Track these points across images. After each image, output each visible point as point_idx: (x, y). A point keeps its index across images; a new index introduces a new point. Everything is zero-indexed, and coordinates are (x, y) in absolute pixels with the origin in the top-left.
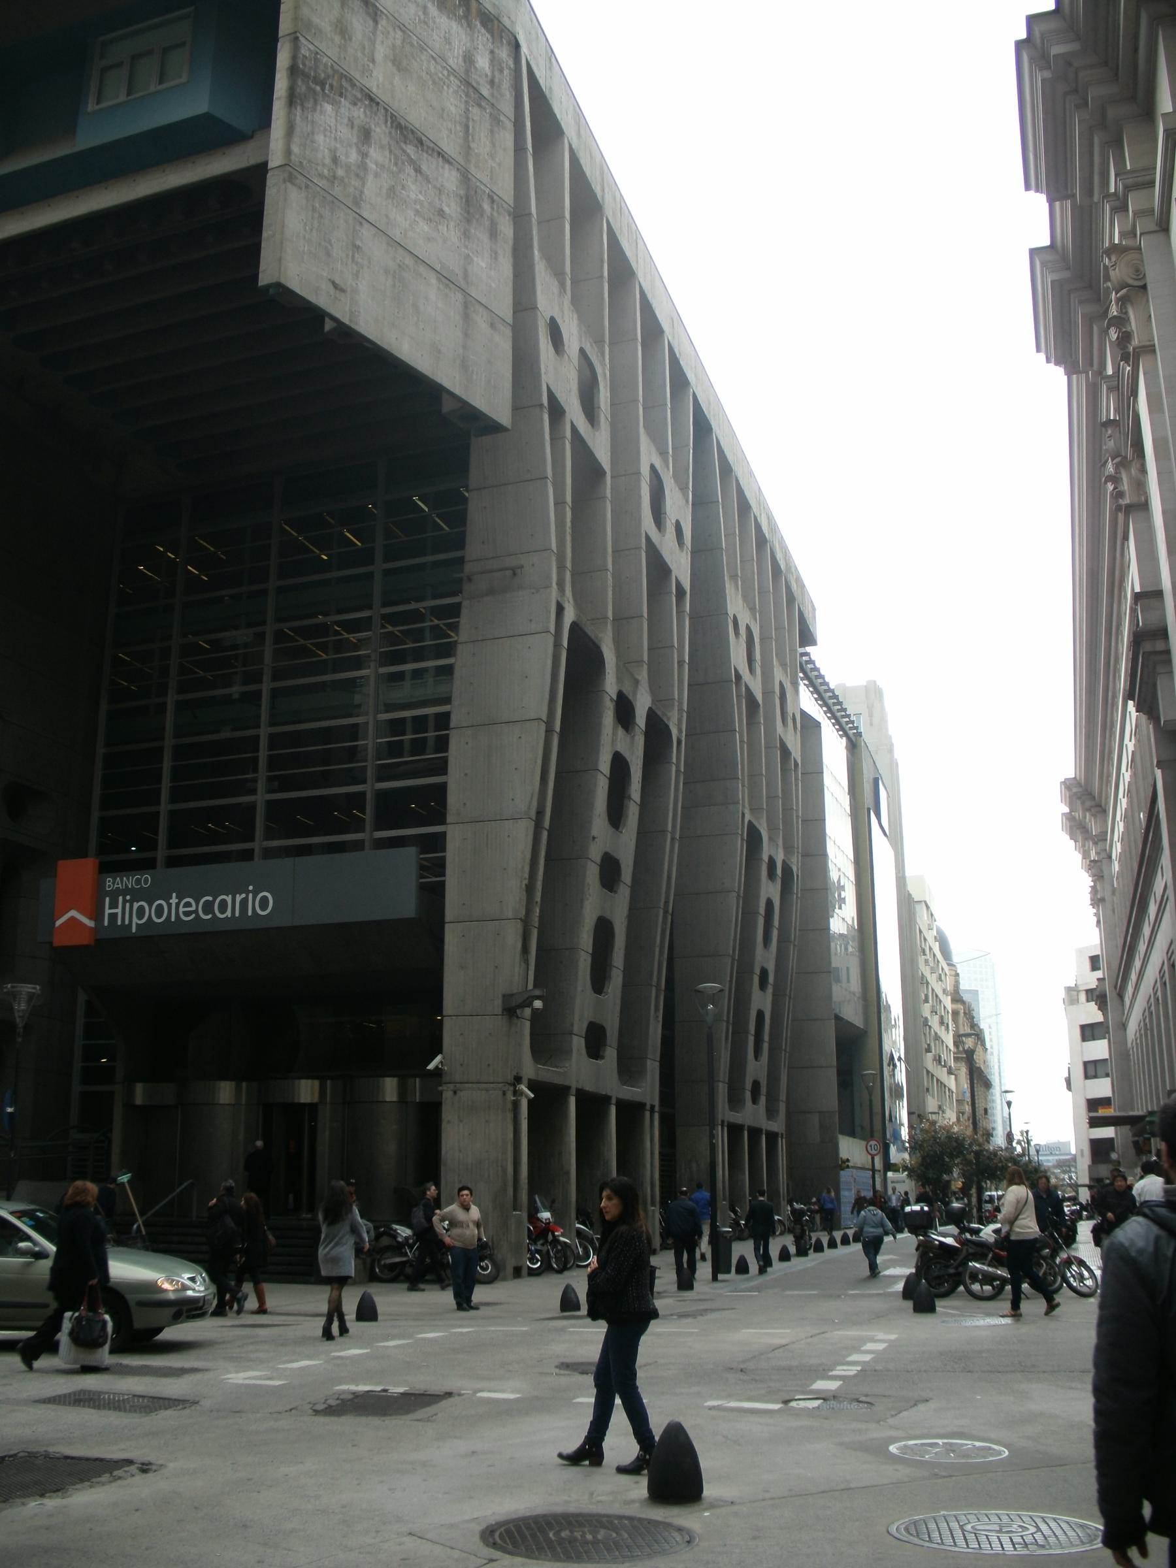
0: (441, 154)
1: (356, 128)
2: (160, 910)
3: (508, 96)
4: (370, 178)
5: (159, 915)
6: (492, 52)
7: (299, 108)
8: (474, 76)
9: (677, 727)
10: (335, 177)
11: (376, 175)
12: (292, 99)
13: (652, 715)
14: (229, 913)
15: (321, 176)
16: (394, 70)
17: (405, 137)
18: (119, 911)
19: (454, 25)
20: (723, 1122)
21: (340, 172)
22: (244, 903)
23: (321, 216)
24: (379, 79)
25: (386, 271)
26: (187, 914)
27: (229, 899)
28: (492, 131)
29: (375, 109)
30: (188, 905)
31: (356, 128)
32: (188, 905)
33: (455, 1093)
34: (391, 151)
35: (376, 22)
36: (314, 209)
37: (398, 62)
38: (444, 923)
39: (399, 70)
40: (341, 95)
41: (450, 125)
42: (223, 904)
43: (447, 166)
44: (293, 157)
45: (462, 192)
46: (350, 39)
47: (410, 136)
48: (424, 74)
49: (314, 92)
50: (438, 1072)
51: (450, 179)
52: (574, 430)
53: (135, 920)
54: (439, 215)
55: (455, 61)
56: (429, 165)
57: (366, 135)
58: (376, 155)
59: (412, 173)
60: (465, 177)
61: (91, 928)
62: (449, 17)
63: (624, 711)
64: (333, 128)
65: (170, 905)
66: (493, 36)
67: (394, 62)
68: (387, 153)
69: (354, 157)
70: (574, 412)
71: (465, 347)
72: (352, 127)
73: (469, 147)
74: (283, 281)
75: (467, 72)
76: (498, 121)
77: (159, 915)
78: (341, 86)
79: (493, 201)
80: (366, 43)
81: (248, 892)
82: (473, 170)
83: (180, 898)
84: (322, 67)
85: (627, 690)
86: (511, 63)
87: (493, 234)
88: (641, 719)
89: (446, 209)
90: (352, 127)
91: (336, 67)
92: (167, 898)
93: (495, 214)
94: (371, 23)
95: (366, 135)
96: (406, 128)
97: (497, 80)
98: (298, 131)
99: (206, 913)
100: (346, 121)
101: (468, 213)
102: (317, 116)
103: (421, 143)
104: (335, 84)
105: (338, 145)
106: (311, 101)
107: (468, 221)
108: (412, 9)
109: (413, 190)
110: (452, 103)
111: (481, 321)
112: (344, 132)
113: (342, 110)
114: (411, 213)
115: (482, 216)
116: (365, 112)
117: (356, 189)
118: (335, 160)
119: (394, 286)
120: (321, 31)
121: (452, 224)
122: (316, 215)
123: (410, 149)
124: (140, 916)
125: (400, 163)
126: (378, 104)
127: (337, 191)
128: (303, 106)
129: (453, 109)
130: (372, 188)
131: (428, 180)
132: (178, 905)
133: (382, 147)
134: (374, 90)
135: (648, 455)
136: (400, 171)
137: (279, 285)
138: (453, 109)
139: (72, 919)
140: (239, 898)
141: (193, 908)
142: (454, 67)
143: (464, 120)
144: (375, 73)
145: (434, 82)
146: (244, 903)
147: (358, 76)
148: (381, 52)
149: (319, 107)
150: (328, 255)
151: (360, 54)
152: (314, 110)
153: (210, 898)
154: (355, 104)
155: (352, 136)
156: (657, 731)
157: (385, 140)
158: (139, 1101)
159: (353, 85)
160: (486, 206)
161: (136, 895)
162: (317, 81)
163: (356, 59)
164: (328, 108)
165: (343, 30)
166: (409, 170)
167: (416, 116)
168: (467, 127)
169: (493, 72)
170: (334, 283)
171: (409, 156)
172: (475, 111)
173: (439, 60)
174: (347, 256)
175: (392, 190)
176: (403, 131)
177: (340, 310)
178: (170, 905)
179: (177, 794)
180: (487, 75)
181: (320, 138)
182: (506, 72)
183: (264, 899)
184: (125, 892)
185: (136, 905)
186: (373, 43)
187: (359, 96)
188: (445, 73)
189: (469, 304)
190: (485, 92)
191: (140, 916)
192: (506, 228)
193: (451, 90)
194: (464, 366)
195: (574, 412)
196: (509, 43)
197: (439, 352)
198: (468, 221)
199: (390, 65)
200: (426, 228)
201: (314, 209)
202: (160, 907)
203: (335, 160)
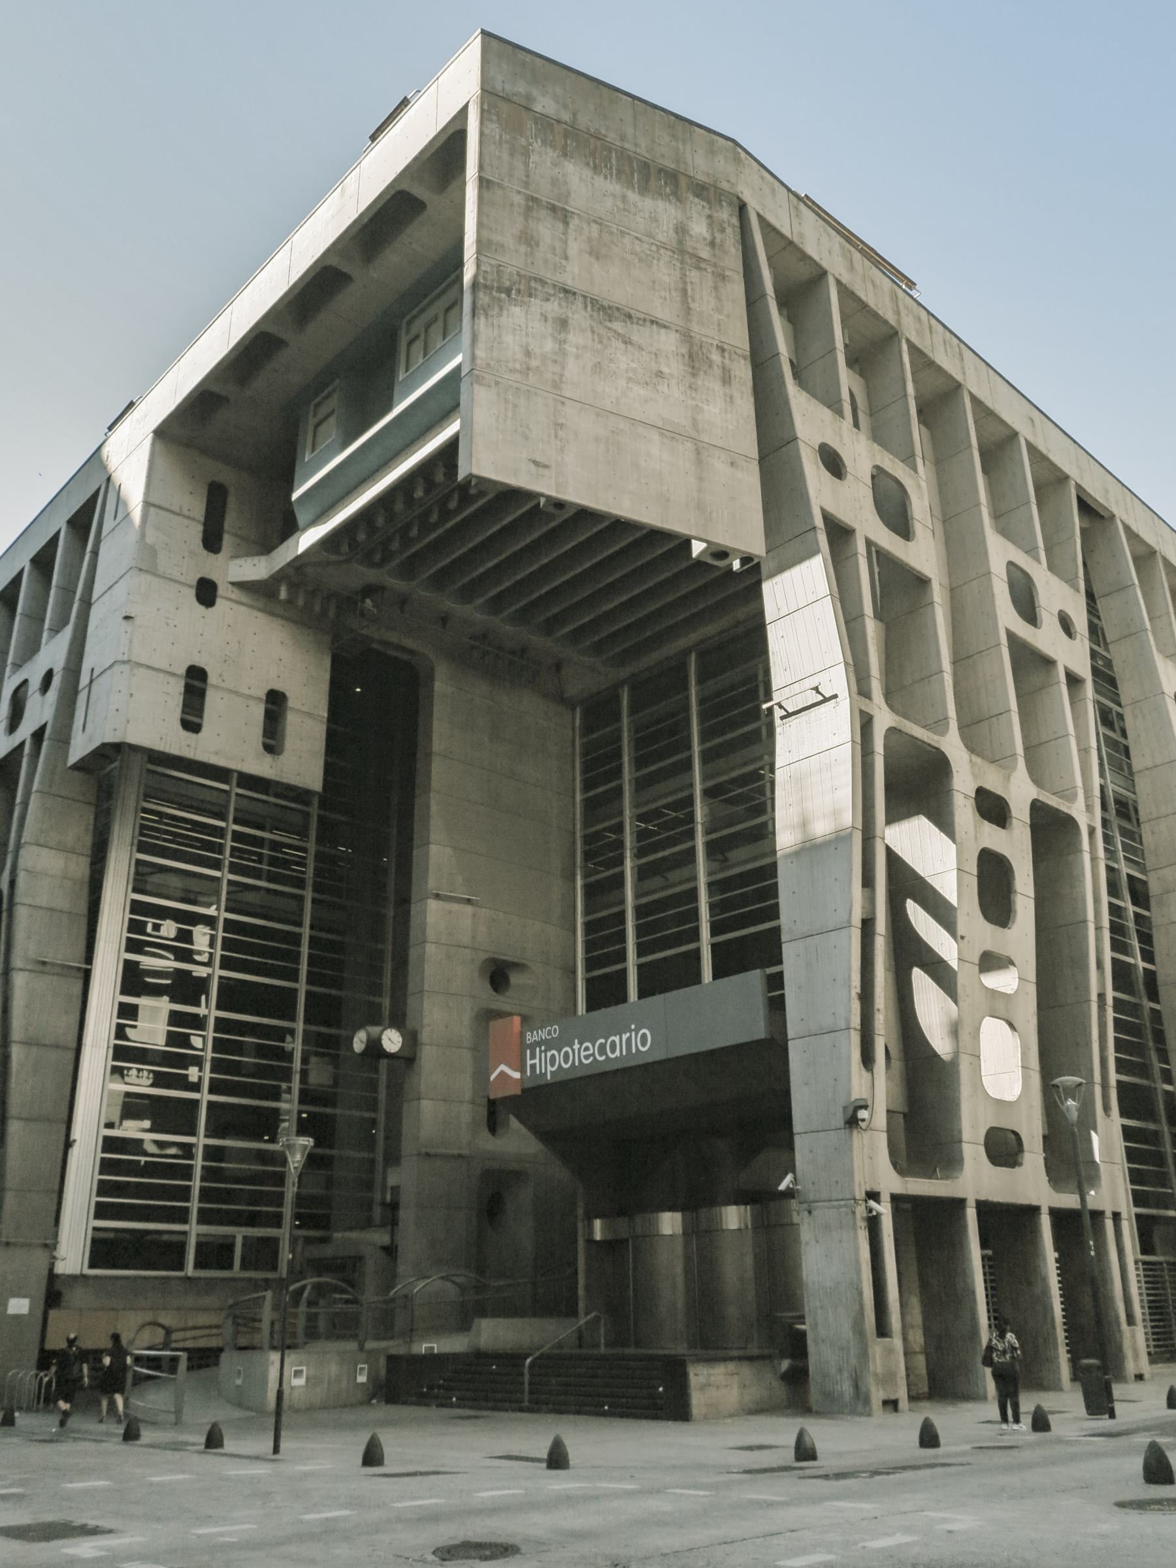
1: (550, 320)
3: (733, 250)
6: (709, 217)
7: (482, 318)
8: (689, 244)
9: (1084, 813)
10: (528, 369)
11: (577, 357)
13: (1037, 808)
14: (618, 1053)
17: (610, 316)
18: (537, 1061)
19: (661, 204)
21: (534, 363)
22: (629, 1040)
23: (516, 406)
24: (574, 274)
25: (597, 440)
26: (587, 1057)
27: (617, 1039)
28: (716, 288)
29: (571, 298)
30: (587, 1049)
31: (550, 320)
32: (587, 1049)
33: (810, 1212)
34: (593, 332)
35: (566, 223)
36: (506, 401)
37: (595, 253)
38: (786, 1041)
39: (597, 258)
40: (530, 295)
41: (663, 294)
42: (613, 1044)
43: (663, 331)
44: (478, 362)
45: (684, 350)
46: (537, 245)
47: (616, 313)
48: (628, 257)
49: (499, 300)
50: (790, 1194)
51: (668, 342)
52: (869, 543)
53: (549, 1068)
54: (657, 376)
55: (665, 233)
56: (638, 334)
57: (563, 324)
59: (622, 346)
60: (687, 336)
61: (516, 1080)
62: (653, 198)
63: (993, 808)
64: (524, 326)
65: (573, 1051)
66: (709, 202)
67: (590, 254)
68: (589, 334)
69: (549, 346)
70: (869, 526)
71: (700, 491)
72: (546, 320)
73: (689, 309)
74: (475, 471)
75: (680, 242)
76: (724, 278)
77: (566, 1062)
78: (530, 288)
79: (723, 350)
80: (557, 244)
81: (630, 1031)
82: (695, 327)
83: (581, 1043)
84: (506, 277)
85: (993, 783)
86: (735, 221)
87: (726, 379)
88: (1020, 813)
89: (666, 370)
90: (546, 320)
91: (522, 272)
92: (571, 1045)
93: (727, 361)
94: (561, 225)
96: (610, 307)
97: (718, 241)
98: (482, 338)
99: (601, 1055)
100: (538, 316)
101: (693, 368)
102: (504, 320)
103: (630, 317)
104: (522, 287)
105: (530, 340)
106: (496, 309)
107: (694, 375)
108: (609, 202)
109: (623, 360)
110: (665, 271)
111: (719, 465)
112: (536, 326)
113: (533, 309)
114: (622, 383)
115: (711, 367)
116: (560, 305)
117: (554, 374)
118: (528, 354)
119: (608, 451)
120: (503, 246)
121: (673, 382)
122: (510, 406)
123: (617, 326)
124: (552, 1065)
125: (605, 341)
126: (575, 294)
128: (486, 315)
129: (667, 279)
130: (572, 369)
131: (640, 348)
132: (579, 1050)
133: (583, 330)
134: (569, 282)
135: (1000, 553)
136: (606, 348)
137: (471, 475)
138: (667, 279)
139: (502, 1072)
140: (625, 1037)
141: (591, 1052)
142: (664, 240)
143: (681, 286)
144: (568, 268)
145: (640, 260)
146: (629, 1040)
147: (549, 275)
148: (573, 248)
149: (505, 312)
150: (527, 438)
151: (549, 256)
152: (500, 315)
153: (603, 1041)
154: (548, 300)
157: (586, 324)
158: (598, 1236)
159: (543, 282)
160: (716, 357)
161: (549, 1044)
162: (499, 290)
163: (546, 261)
164: (516, 310)
165: (528, 239)
168: (685, 291)
169: (713, 234)
170: (535, 462)
171: (615, 332)
172: (693, 275)
173: (645, 239)
174: (549, 435)
175: (597, 367)
176: (604, 311)
177: (545, 486)
178: (573, 1051)
179: (641, 950)
180: (705, 239)
181: (509, 339)
182: (729, 230)
183: (644, 1036)
184: (538, 1044)
185: (549, 1054)
186: (566, 242)
187: (552, 292)
188: (654, 248)
189: (700, 452)
190: (705, 253)
191: (552, 1065)
192: (743, 372)
193: (662, 262)
194: (700, 507)
196: (730, 204)
197: (668, 500)
198: (694, 375)
199: (587, 256)
200: (642, 392)
201: (506, 401)
202: (566, 1053)
203: (528, 354)
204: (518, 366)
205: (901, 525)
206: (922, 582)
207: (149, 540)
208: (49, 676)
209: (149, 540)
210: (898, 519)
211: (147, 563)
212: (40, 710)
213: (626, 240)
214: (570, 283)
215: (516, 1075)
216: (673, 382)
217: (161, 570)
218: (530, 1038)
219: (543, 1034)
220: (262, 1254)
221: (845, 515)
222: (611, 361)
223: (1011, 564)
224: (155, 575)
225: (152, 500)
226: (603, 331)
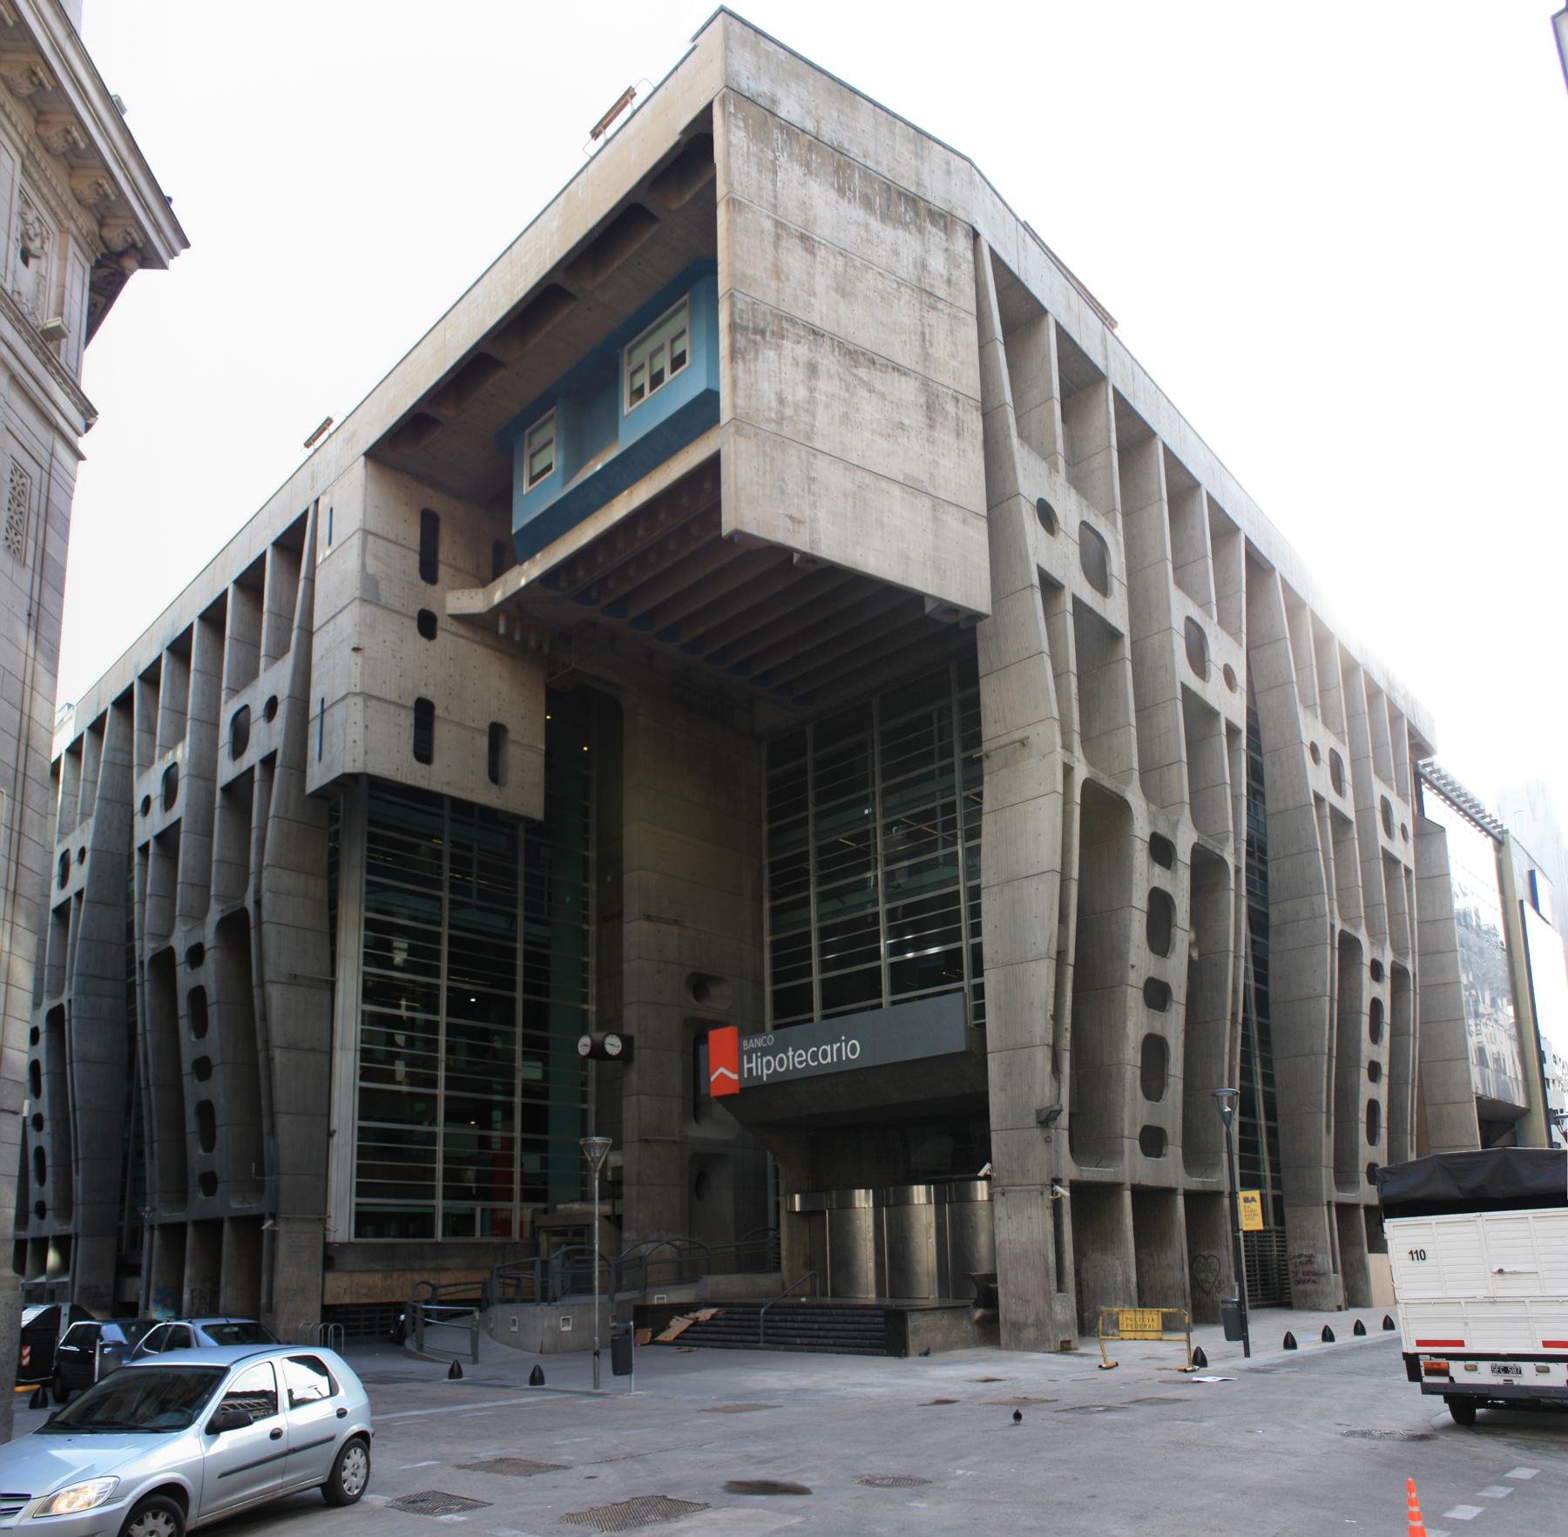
0: (897, 368)
2: (781, 1060)
4: (821, 410)
5: (781, 1065)
11: (827, 406)
12: (734, 354)
15: (769, 420)
16: (838, 297)
17: (856, 361)
20: (1329, 1203)
21: (789, 412)
24: (823, 310)
37: (843, 290)
39: (843, 296)
47: (861, 359)
48: (872, 295)
52: (1077, 602)
57: (812, 369)
58: (823, 385)
67: (837, 290)
68: (837, 382)
69: (802, 393)
70: (1076, 584)
77: (781, 1065)
83: (794, 1051)
92: (786, 1052)
95: (812, 369)
123: (862, 372)
127: (787, 430)
130: (822, 419)
133: (830, 377)
134: (818, 323)
138: (906, 321)
148: (822, 283)
155: (800, 374)
156: (1206, 866)
157: (834, 369)
159: (792, 321)
161: (765, 1051)
166: (863, 392)
167: (865, 338)
175: (845, 419)
176: (854, 355)
193: (902, 302)
195: (1076, 584)
199: (833, 293)
204: (774, 416)
205: (1100, 581)
206: (1114, 635)
207: (370, 570)
208: (272, 706)
209: (370, 570)
210: (1098, 575)
211: (370, 593)
212: (266, 738)
213: (870, 276)
214: (815, 319)
215: (735, 1077)
216: (913, 434)
217: (383, 600)
218: (746, 1045)
219: (758, 1042)
220: (501, 1226)
221: (1056, 573)
222: (857, 410)
223: (1189, 619)
224: (377, 604)
225: (370, 527)
226: (848, 378)
